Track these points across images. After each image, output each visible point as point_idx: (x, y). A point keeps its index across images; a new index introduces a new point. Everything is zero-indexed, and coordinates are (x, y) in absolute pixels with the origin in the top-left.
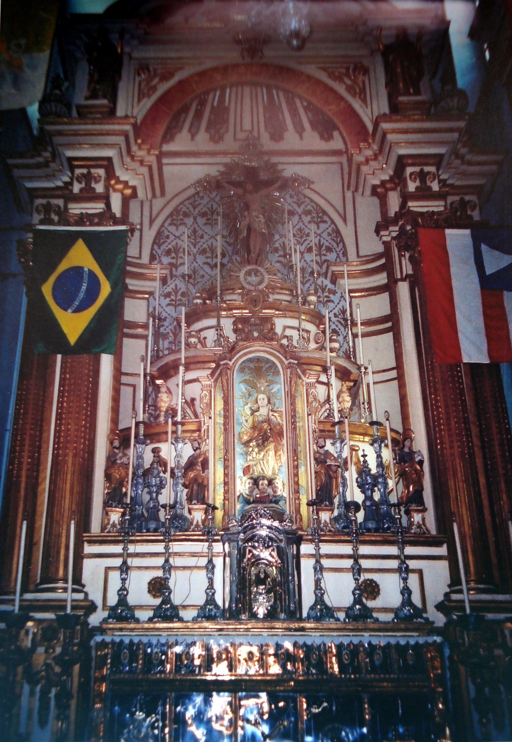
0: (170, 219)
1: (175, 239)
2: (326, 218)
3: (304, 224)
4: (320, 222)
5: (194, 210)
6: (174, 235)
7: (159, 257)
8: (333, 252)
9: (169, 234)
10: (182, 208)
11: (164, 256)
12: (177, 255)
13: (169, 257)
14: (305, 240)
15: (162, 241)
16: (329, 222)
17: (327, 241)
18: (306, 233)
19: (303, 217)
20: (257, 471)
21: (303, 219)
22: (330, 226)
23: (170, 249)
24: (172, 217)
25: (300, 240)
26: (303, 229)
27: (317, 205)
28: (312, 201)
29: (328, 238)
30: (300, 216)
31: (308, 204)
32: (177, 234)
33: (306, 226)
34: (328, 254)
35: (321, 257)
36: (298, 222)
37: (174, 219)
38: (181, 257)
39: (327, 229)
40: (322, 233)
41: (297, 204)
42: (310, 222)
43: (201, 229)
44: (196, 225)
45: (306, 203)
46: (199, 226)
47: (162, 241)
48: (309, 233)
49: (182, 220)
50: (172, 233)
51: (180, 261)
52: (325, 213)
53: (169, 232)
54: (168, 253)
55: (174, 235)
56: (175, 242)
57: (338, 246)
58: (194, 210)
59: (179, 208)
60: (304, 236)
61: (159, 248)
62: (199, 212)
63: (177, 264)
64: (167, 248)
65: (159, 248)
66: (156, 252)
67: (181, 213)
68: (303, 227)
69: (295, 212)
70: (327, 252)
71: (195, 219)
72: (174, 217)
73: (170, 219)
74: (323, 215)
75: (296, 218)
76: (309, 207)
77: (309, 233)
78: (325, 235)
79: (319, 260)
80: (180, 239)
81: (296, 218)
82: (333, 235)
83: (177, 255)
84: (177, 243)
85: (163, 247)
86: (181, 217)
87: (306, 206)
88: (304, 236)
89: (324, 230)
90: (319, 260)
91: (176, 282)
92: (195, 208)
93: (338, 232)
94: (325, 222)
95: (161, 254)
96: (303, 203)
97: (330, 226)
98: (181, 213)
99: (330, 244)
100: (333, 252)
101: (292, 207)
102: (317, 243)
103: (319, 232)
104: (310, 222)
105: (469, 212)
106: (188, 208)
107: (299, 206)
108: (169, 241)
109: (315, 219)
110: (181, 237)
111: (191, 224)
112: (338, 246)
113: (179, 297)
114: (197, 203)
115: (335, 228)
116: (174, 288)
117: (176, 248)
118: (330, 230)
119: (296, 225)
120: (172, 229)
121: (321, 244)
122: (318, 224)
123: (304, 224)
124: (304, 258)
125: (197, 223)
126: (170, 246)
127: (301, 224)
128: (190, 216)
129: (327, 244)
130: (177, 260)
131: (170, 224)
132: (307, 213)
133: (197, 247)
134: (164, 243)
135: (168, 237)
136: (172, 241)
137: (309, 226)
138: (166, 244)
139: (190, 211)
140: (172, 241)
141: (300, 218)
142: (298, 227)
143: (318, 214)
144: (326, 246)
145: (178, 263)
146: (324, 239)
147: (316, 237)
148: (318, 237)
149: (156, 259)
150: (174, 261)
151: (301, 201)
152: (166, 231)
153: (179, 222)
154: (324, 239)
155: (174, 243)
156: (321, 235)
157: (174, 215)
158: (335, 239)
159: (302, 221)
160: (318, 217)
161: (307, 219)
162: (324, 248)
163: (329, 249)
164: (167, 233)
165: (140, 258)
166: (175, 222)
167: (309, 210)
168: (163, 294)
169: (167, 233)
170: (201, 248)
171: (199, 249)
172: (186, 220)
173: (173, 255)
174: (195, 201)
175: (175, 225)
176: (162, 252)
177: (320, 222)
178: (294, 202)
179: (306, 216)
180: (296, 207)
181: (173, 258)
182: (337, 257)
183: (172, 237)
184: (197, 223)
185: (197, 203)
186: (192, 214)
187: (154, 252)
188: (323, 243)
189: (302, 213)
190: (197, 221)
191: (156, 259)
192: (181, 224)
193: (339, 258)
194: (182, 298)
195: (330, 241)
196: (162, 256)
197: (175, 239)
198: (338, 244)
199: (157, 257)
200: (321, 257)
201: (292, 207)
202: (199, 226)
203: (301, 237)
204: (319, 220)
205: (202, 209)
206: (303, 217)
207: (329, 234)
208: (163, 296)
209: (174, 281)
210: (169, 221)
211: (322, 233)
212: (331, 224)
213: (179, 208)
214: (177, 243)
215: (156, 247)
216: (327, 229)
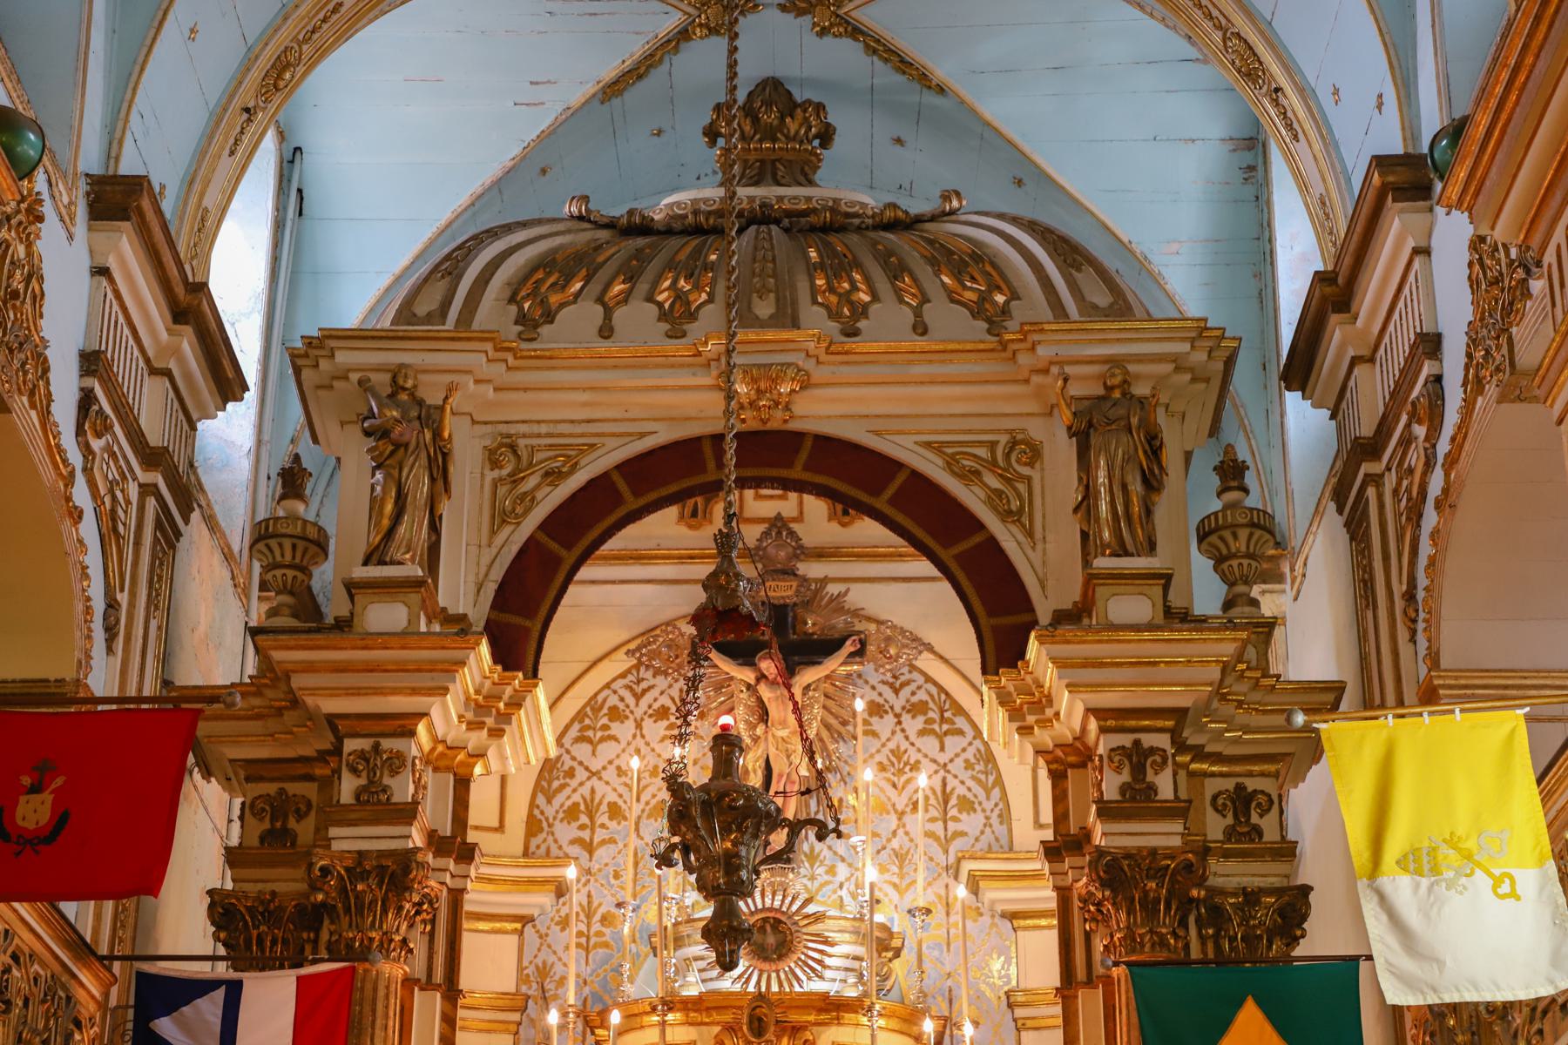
0: (576, 726)
1: (589, 778)
2: (961, 722)
3: (907, 738)
4: (946, 734)
5: (637, 705)
6: (587, 769)
7: (550, 826)
8: (975, 811)
9: (575, 764)
10: (605, 700)
11: (562, 820)
12: (592, 819)
13: (575, 825)
14: (908, 781)
15: (556, 784)
16: (970, 732)
17: (963, 783)
18: (912, 761)
19: (906, 718)
21: (904, 725)
22: (970, 744)
23: (576, 805)
24: (581, 721)
25: (895, 779)
26: (906, 751)
27: (941, 689)
28: (929, 679)
29: (965, 775)
30: (897, 716)
31: (919, 688)
32: (595, 765)
33: (913, 744)
34: (964, 816)
35: (945, 822)
36: (893, 733)
37: (588, 727)
38: (603, 826)
39: (964, 750)
40: (951, 761)
41: (891, 685)
42: (922, 733)
43: (653, 750)
44: (639, 742)
45: (913, 687)
46: (647, 744)
47: (556, 784)
48: (918, 762)
49: (605, 727)
50: (581, 763)
51: (600, 835)
52: (960, 710)
53: (574, 759)
54: (571, 813)
55: (587, 769)
56: (588, 785)
57: (988, 798)
58: (637, 705)
59: (600, 698)
60: (908, 768)
61: (549, 802)
62: (650, 707)
63: (592, 840)
64: (568, 803)
65: (549, 802)
66: (542, 813)
67: (605, 711)
68: (905, 745)
69: (887, 707)
70: (960, 812)
71: (639, 726)
72: (587, 721)
73: (576, 726)
74: (954, 715)
75: (890, 719)
76: (922, 696)
77: (918, 762)
78: (957, 767)
79: (941, 833)
80: (600, 779)
81: (890, 719)
82: (977, 768)
83: (592, 819)
84: (593, 791)
85: (558, 800)
86: (605, 721)
87: (913, 693)
88: (908, 768)
89: (957, 755)
90: (941, 833)
91: (591, 887)
92: (638, 697)
93: (988, 758)
94: (960, 732)
95: (555, 818)
96: (907, 683)
97: (970, 744)
98: (605, 711)
99: (969, 789)
100: (975, 811)
101: (880, 694)
102: (939, 790)
103: (943, 758)
104: (922, 733)
106: (622, 699)
107: (896, 692)
108: (574, 783)
109: (936, 727)
110: (603, 774)
111: (630, 738)
112: (988, 798)
113: (596, 927)
114: (644, 685)
115: (982, 749)
116: (585, 903)
117: (592, 800)
118: (970, 754)
119: (888, 740)
120: (582, 751)
121: (948, 789)
122: (941, 738)
123: (907, 738)
124: (904, 826)
125: (643, 736)
126: (576, 798)
127: (899, 736)
128: (627, 718)
129: (961, 790)
130: (593, 831)
131: (578, 740)
132: (917, 709)
133: (644, 798)
134: (563, 786)
135: (571, 773)
136: (581, 784)
137: (919, 742)
138: (567, 791)
139: (628, 706)
140: (581, 784)
141: (899, 723)
142: (891, 745)
143: (942, 711)
144: (959, 796)
145: (596, 840)
146: (956, 777)
147: (936, 772)
148: (942, 773)
149: (541, 830)
150: (586, 835)
151: (903, 678)
152: (566, 757)
153: (599, 734)
154: (956, 777)
155: (585, 790)
156: (950, 767)
157: (586, 715)
158: (983, 777)
159: (903, 730)
160: (943, 720)
161: (913, 725)
162: (953, 801)
163: (967, 805)
164: (568, 763)
165: (500, 828)
166: (590, 733)
167: (921, 701)
168: (557, 918)
169: (568, 763)
170: (653, 802)
171: (647, 803)
172: (616, 728)
173: (584, 819)
174: (639, 681)
175: (590, 741)
176: (557, 812)
177: (946, 734)
178: (884, 682)
179: (913, 717)
180: (888, 693)
181: (582, 827)
182: (985, 825)
183: (581, 774)
184: (643, 736)
185: (644, 685)
186: (632, 712)
187: (536, 812)
188: (953, 789)
189: (903, 708)
190: (644, 732)
191: (541, 830)
192: (602, 740)
193: (991, 826)
194: (604, 929)
195: (970, 783)
196: (557, 822)
197: (589, 778)
198: (988, 792)
199: (545, 824)
200: (945, 822)
201: (880, 694)
202: (647, 744)
203: (901, 772)
204: (945, 727)
205: (655, 700)
206: (906, 718)
207: (968, 765)
208: (557, 924)
209: (585, 885)
210: (574, 732)
211: (951, 761)
212: (974, 738)
213: (600, 698)
214: (593, 791)
215: (541, 800)
216: (964, 750)
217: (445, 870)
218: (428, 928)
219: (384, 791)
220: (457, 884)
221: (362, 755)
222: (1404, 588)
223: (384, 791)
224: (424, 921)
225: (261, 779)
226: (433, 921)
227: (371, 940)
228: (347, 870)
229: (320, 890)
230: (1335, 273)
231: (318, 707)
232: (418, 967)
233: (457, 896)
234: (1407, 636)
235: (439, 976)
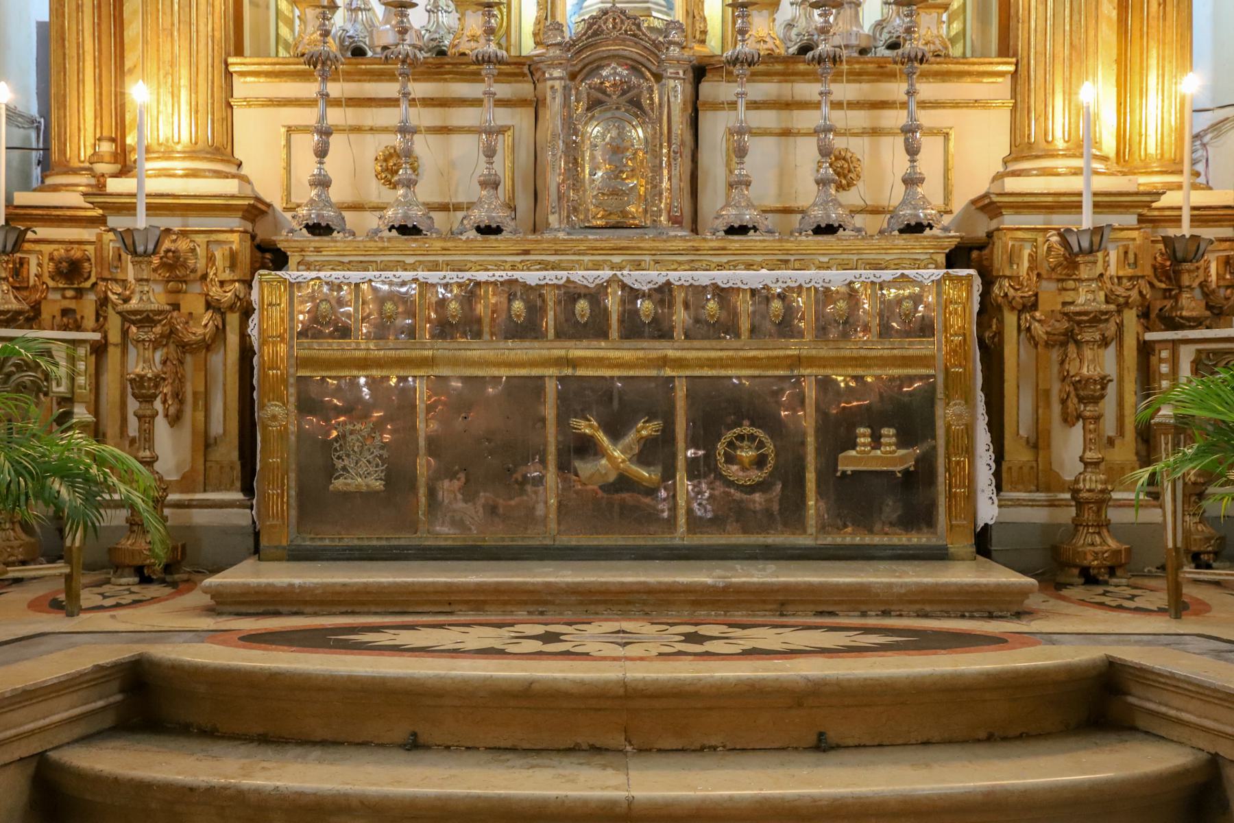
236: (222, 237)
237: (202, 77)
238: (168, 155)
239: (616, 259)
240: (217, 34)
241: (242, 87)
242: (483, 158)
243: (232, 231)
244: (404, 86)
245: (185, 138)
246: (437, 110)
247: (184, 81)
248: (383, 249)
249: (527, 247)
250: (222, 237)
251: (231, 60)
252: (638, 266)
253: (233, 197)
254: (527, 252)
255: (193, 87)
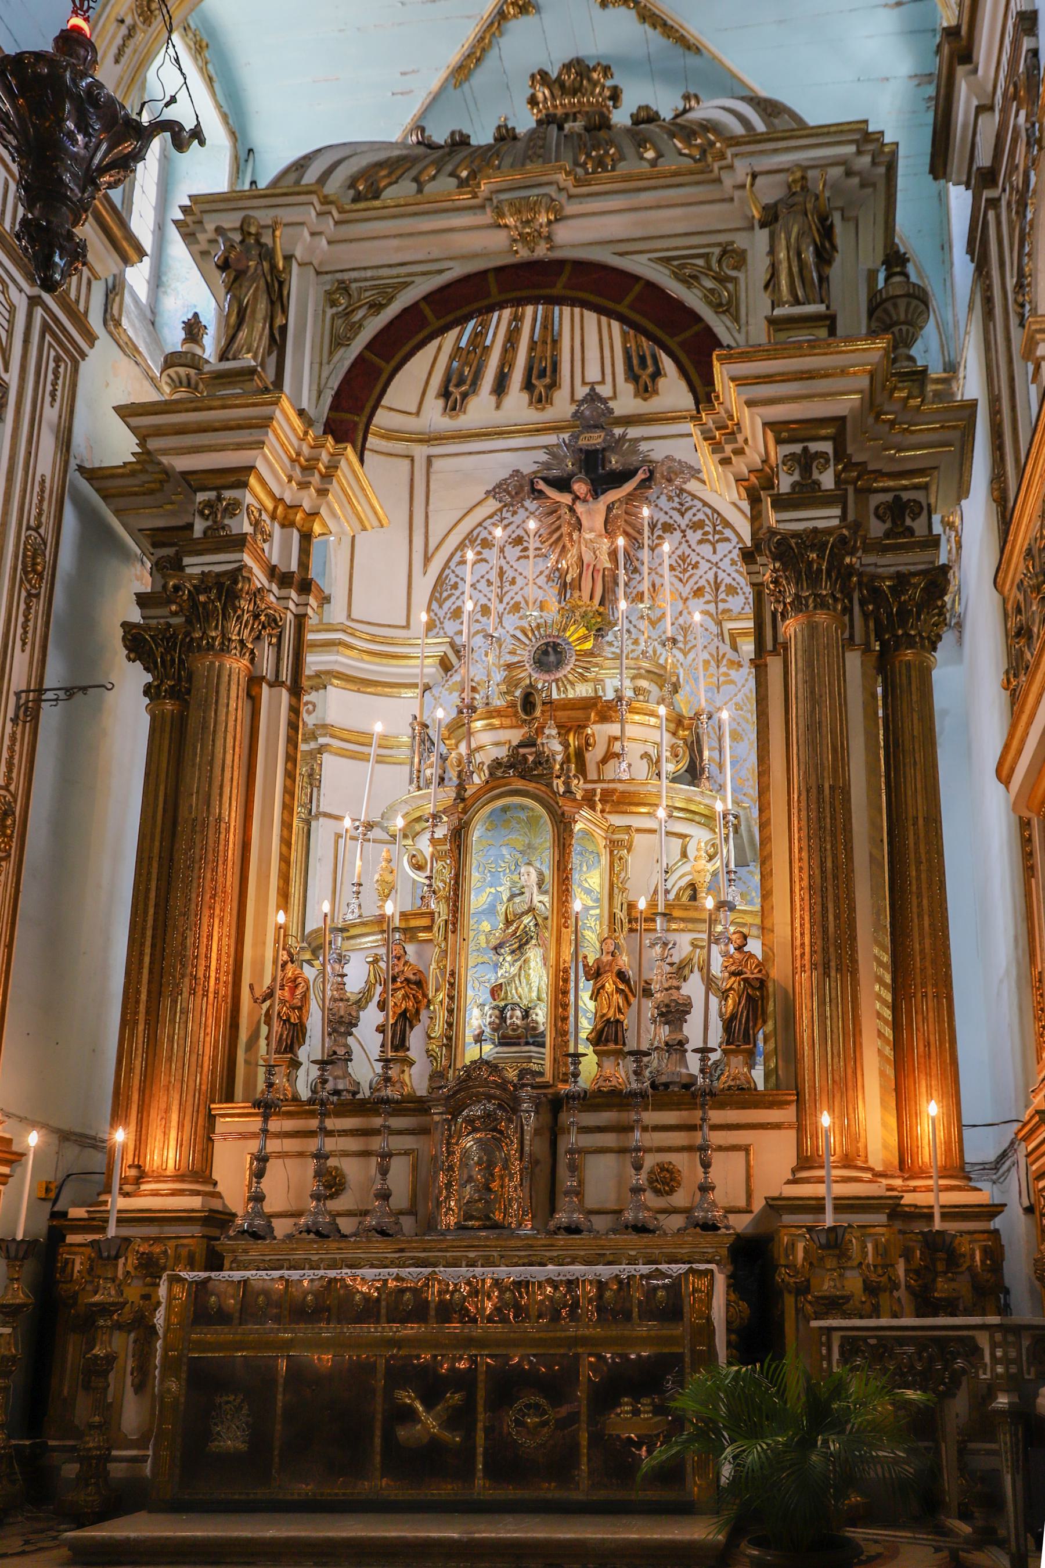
20: (513, 995)
105: (908, 522)
217: (288, 598)
218: (274, 640)
219: (223, 528)
220: (301, 610)
221: (209, 504)
222: (1015, 280)
223: (223, 528)
224: (270, 635)
225: (164, 545)
226: (280, 638)
227: (214, 639)
228: (194, 586)
229: (175, 603)
230: (958, 27)
231: (173, 467)
232: (267, 668)
233: (300, 619)
234: (1017, 321)
235: (286, 675)
236: (186, 1241)
237: (188, 1118)
238: (160, 1178)
239: (472, 1255)
240: (204, 1087)
241: (222, 1125)
242: (379, 1176)
243: (193, 1237)
244: (322, 1122)
245: (171, 1164)
246: (361, 1139)
247: (174, 1123)
248: (293, 1249)
249: (403, 1246)
250: (186, 1241)
251: (213, 1106)
252: (488, 1262)
253: (193, 1211)
254: (402, 1250)
255: (181, 1126)
